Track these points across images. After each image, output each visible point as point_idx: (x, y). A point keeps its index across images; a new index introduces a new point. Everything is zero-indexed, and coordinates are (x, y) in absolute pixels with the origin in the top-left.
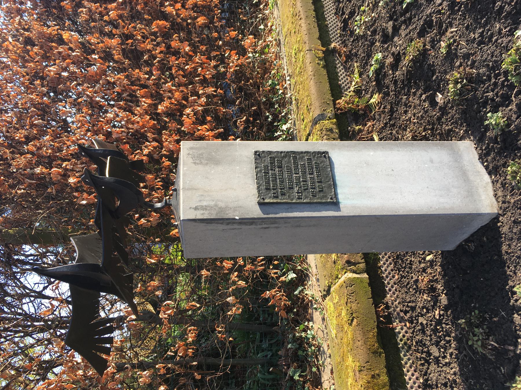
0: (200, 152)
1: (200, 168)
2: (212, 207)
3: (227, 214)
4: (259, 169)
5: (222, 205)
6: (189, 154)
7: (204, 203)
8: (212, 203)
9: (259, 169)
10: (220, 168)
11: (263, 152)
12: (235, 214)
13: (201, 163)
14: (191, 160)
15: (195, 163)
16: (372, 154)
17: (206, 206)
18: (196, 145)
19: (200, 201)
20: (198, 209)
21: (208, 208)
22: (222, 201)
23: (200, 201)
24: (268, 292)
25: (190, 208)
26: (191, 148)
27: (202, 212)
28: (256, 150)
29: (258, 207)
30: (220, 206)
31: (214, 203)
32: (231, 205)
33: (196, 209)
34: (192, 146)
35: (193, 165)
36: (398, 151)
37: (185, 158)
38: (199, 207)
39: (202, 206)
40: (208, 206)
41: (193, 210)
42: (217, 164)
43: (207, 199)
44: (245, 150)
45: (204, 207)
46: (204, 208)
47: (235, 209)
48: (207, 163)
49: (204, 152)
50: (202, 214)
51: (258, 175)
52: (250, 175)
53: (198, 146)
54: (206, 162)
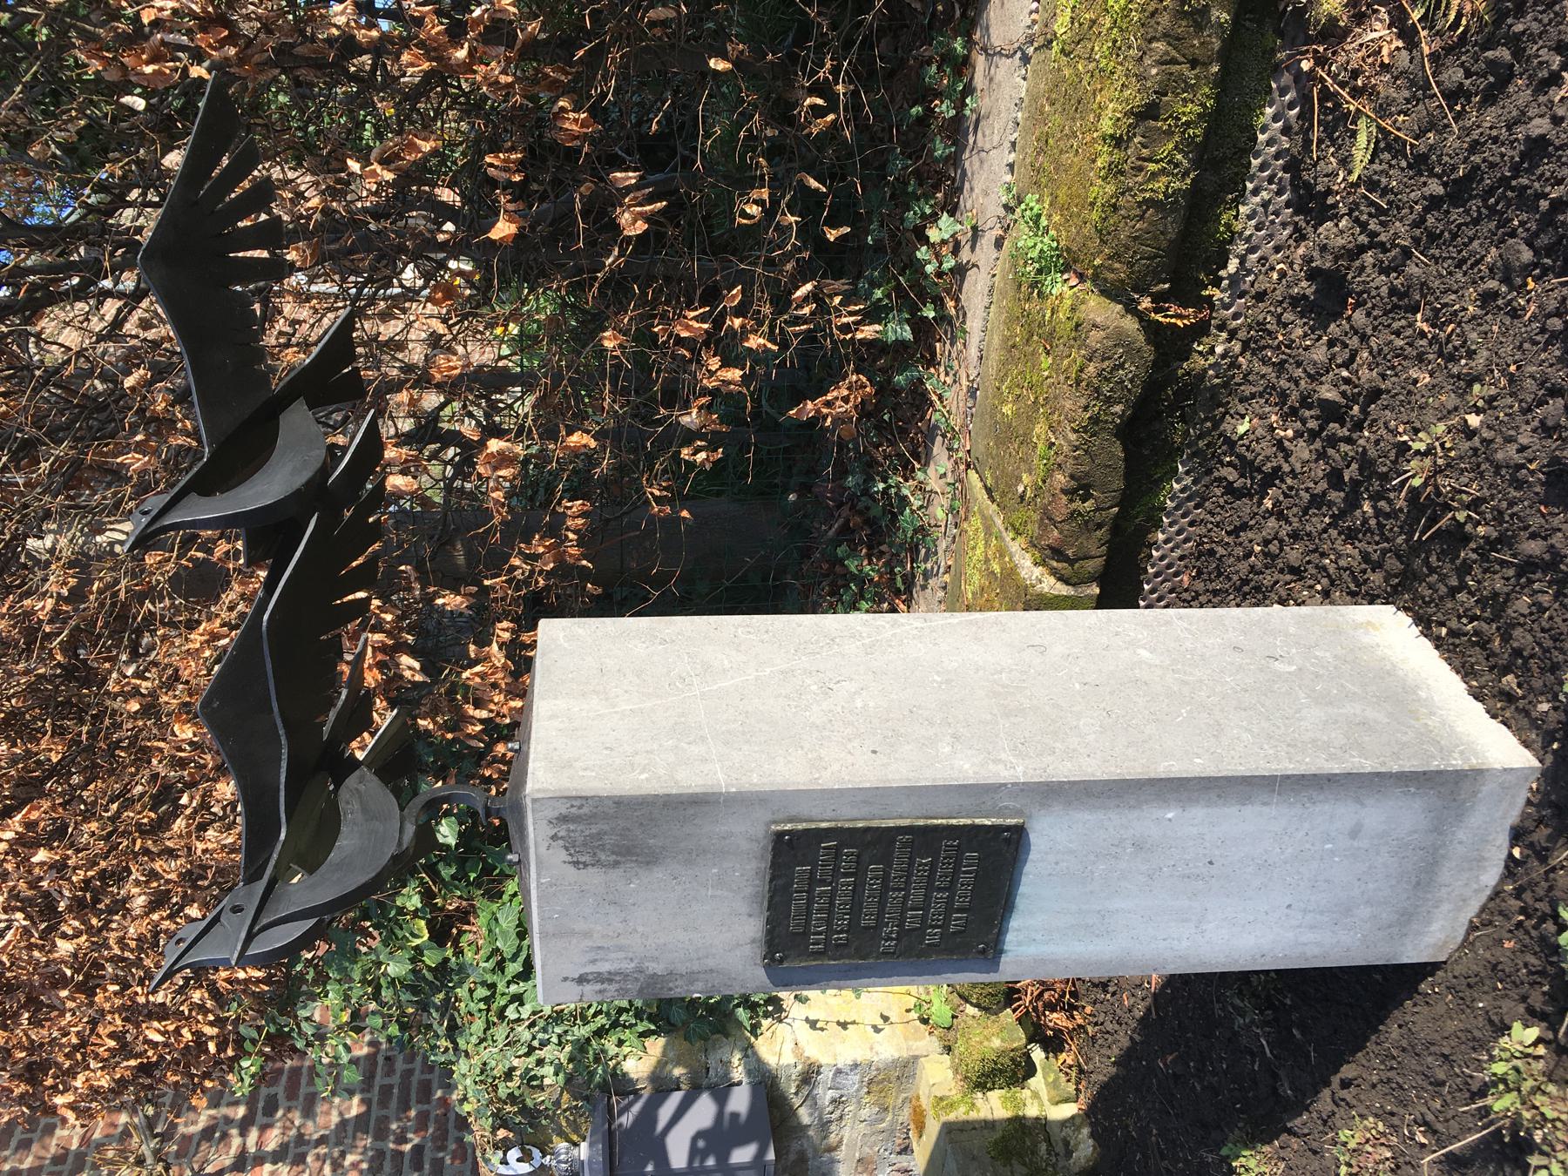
1: (594, 878)
4: (780, 882)
6: (554, 838)
7: (604, 967)
9: (780, 882)
10: (659, 873)
13: (597, 863)
14: (563, 855)
15: (576, 863)
16: (1170, 815)
18: (580, 807)
20: (588, 981)
22: (655, 959)
23: (594, 962)
24: (810, 405)
25: (566, 979)
27: (598, 987)
29: (761, 972)
30: (651, 971)
33: (582, 980)
34: (564, 811)
35: (571, 869)
36: (1265, 804)
37: (543, 850)
40: (617, 974)
42: (648, 863)
43: (613, 955)
47: (692, 977)
48: (616, 864)
49: (606, 827)
51: (777, 899)
52: (749, 890)
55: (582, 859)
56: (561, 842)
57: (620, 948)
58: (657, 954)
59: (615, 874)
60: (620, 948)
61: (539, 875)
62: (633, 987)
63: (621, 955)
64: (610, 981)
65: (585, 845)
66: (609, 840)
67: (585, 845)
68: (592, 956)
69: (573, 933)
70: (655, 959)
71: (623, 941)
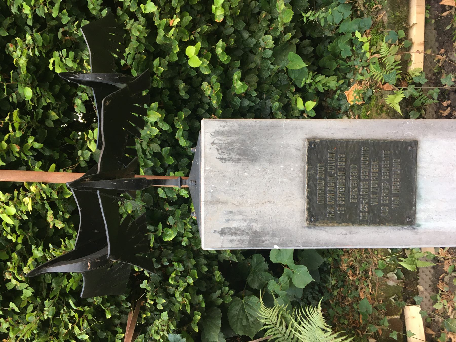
0: (229, 140)
2: (243, 231)
3: (263, 242)
5: (257, 227)
6: (213, 143)
7: (234, 225)
8: (244, 225)
10: (257, 167)
11: (322, 141)
12: (273, 241)
13: (230, 159)
14: (216, 153)
15: (221, 159)
17: (235, 228)
18: (224, 127)
19: (228, 221)
20: (225, 233)
21: (239, 232)
22: (256, 221)
23: (228, 221)
26: (218, 133)
27: (230, 238)
28: (309, 136)
30: (254, 229)
31: (246, 224)
32: (270, 227)
33: (223, 232)
34: (217, 129)
35: (219, 161)
37: (207, 150)
38: (226, 231)
39: (231, 229)
41: (218, 235)
42: (253, 160)
43: (237, 217)
44: (295, 134)
45: (234, 231)
46: (233, 232)
48: (239, 160)
50: (231, 241)
53: (226, 129)
54: (238, 156)
55: (224, 157)
56: (215, 146)
57: (240, 213)
58: (257, 217)
59: (239, 167)
60: (240, 213)
61: (205, 165)
62: (247, 238)
63: (240, 217)
64: (236, 234)
65: (225, 148)
66: (237, 146)
67: (225, 148)
68: (226, 217)
69: (218, 202)
70: (256, 221)
71: (242, 209)
